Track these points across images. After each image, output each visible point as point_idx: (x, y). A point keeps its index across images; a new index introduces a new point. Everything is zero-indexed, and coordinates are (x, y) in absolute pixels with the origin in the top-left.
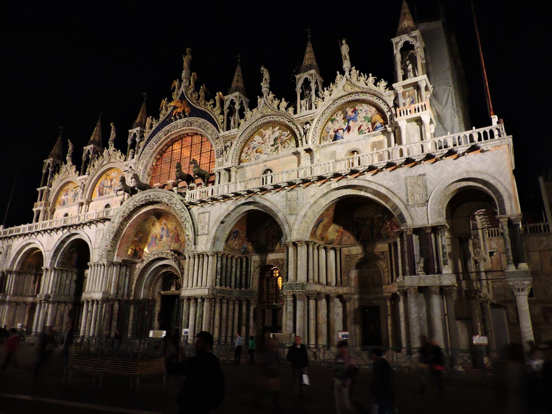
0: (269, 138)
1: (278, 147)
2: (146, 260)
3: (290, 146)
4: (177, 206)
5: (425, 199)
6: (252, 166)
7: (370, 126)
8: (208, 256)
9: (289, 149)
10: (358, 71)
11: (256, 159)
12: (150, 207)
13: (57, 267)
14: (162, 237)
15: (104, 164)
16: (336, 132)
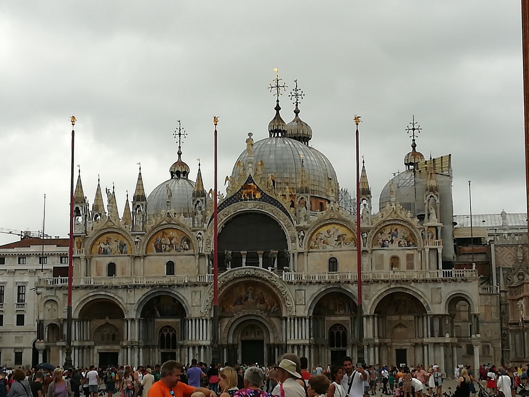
0: (334, 234)
1: (341, 243)
2: (237, 316)
3: (350, 244)
4: (276, 282)
5: (440, 300)
6: (320, 252)
7: (406, 243)
8: (305, 319)
9: (350, 246)
10: (401, 207)
12: (246, 279)
13: (140, 317)
14: (247, 298)
15: (162, 224)
16: (384, 241)
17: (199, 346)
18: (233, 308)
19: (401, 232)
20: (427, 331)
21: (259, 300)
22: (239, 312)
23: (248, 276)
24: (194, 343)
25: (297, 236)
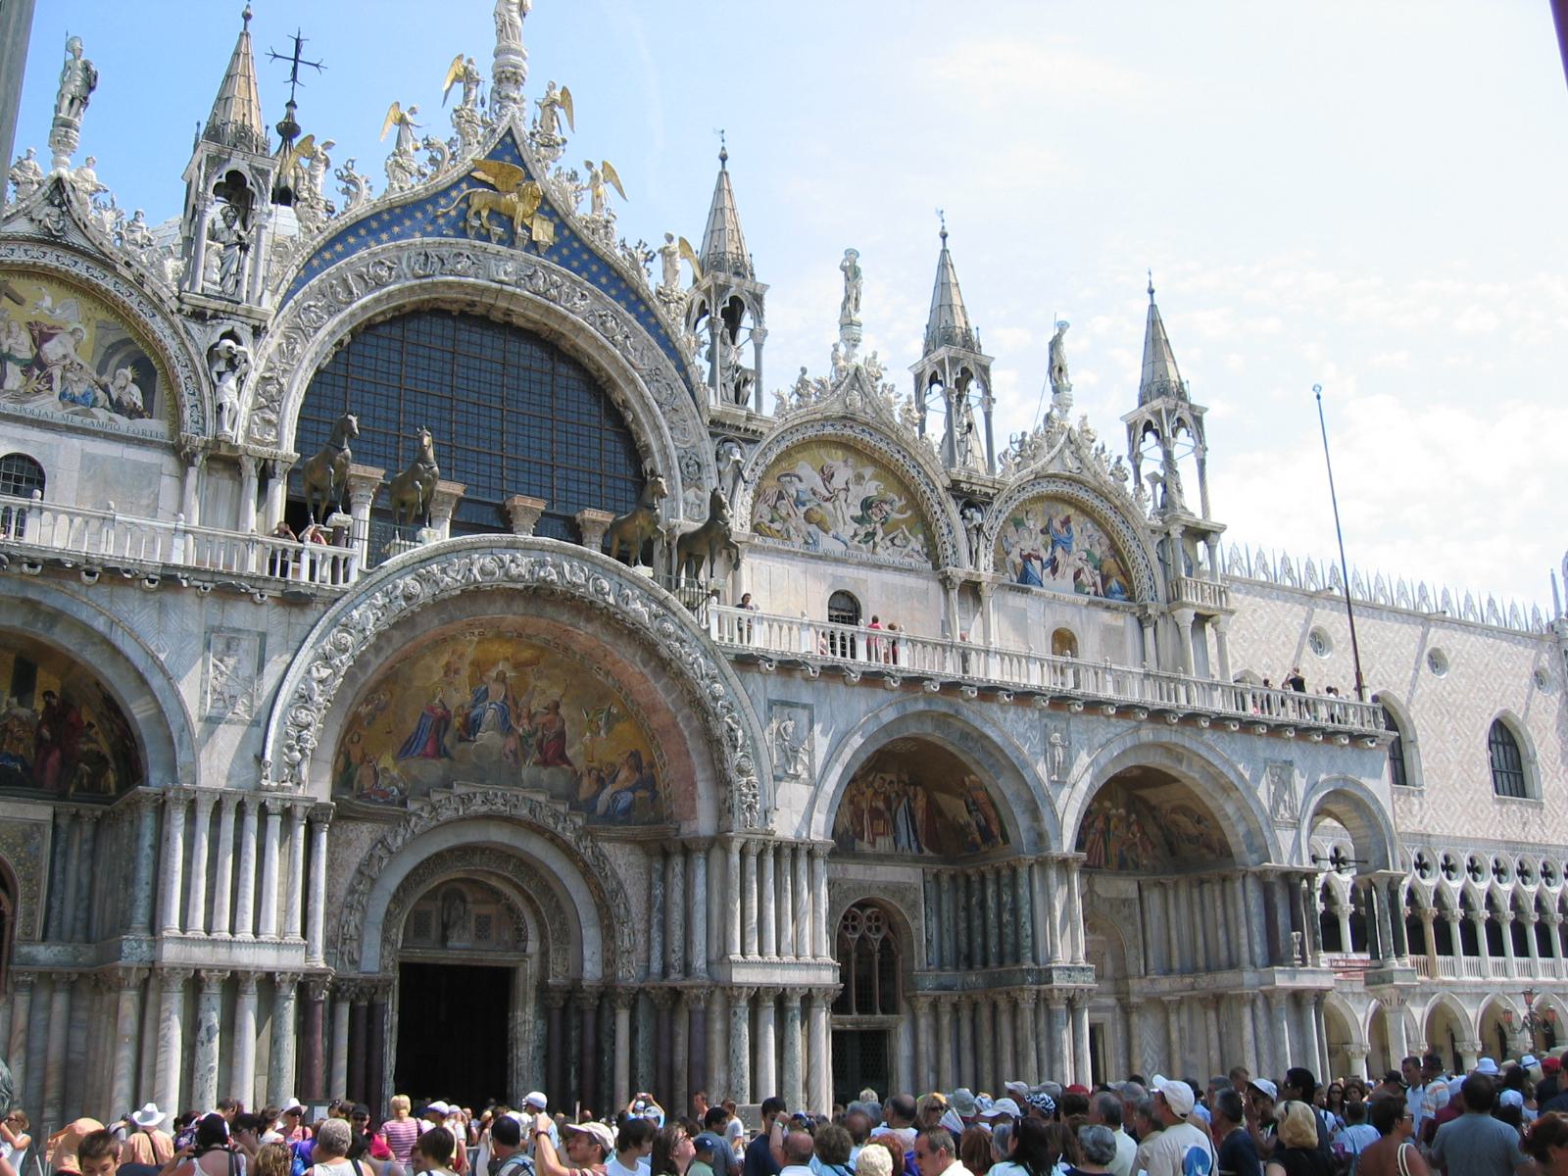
0: (847, 490)
1: (871, 535)
3: (909, 548)
7: (1098, 579)
9: (908, 555)
11: (806, 542)
14: (471, 726)
16: (1027, 558)
17: (234, 973)
18: (395, 773)
19: (1083, 537)
20: (1251, 938)
21: (532, 741)
22: (436, 797)
23: (539, 594)
24: (201, 956)
25: (711, 458)
